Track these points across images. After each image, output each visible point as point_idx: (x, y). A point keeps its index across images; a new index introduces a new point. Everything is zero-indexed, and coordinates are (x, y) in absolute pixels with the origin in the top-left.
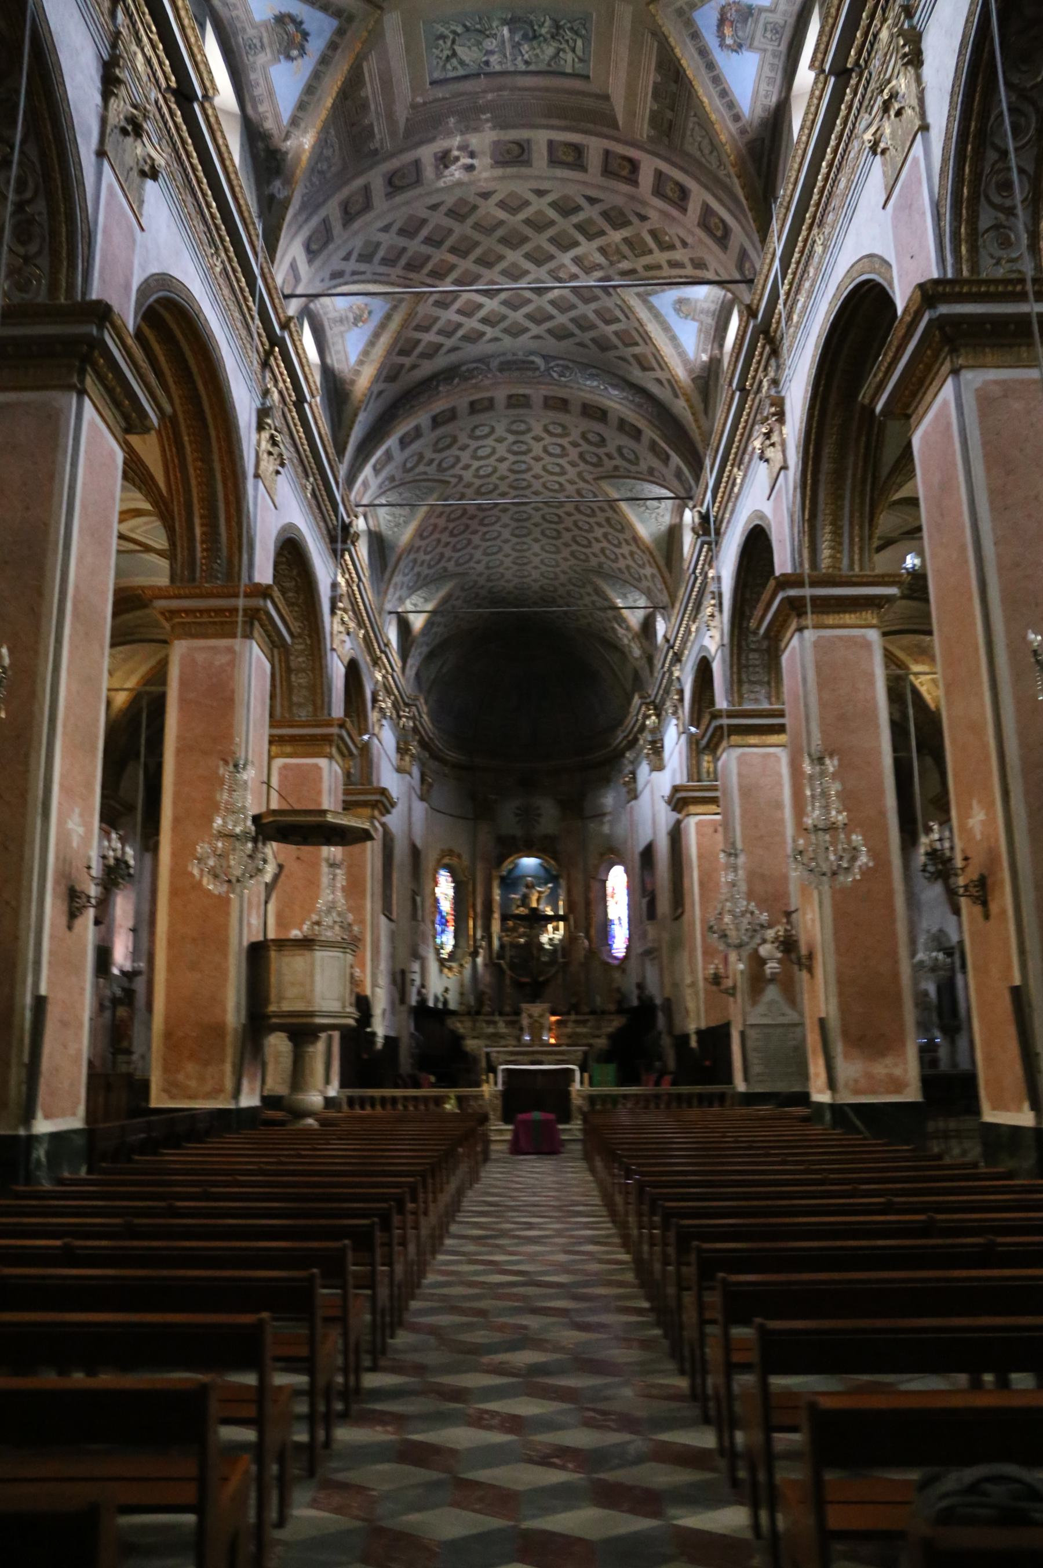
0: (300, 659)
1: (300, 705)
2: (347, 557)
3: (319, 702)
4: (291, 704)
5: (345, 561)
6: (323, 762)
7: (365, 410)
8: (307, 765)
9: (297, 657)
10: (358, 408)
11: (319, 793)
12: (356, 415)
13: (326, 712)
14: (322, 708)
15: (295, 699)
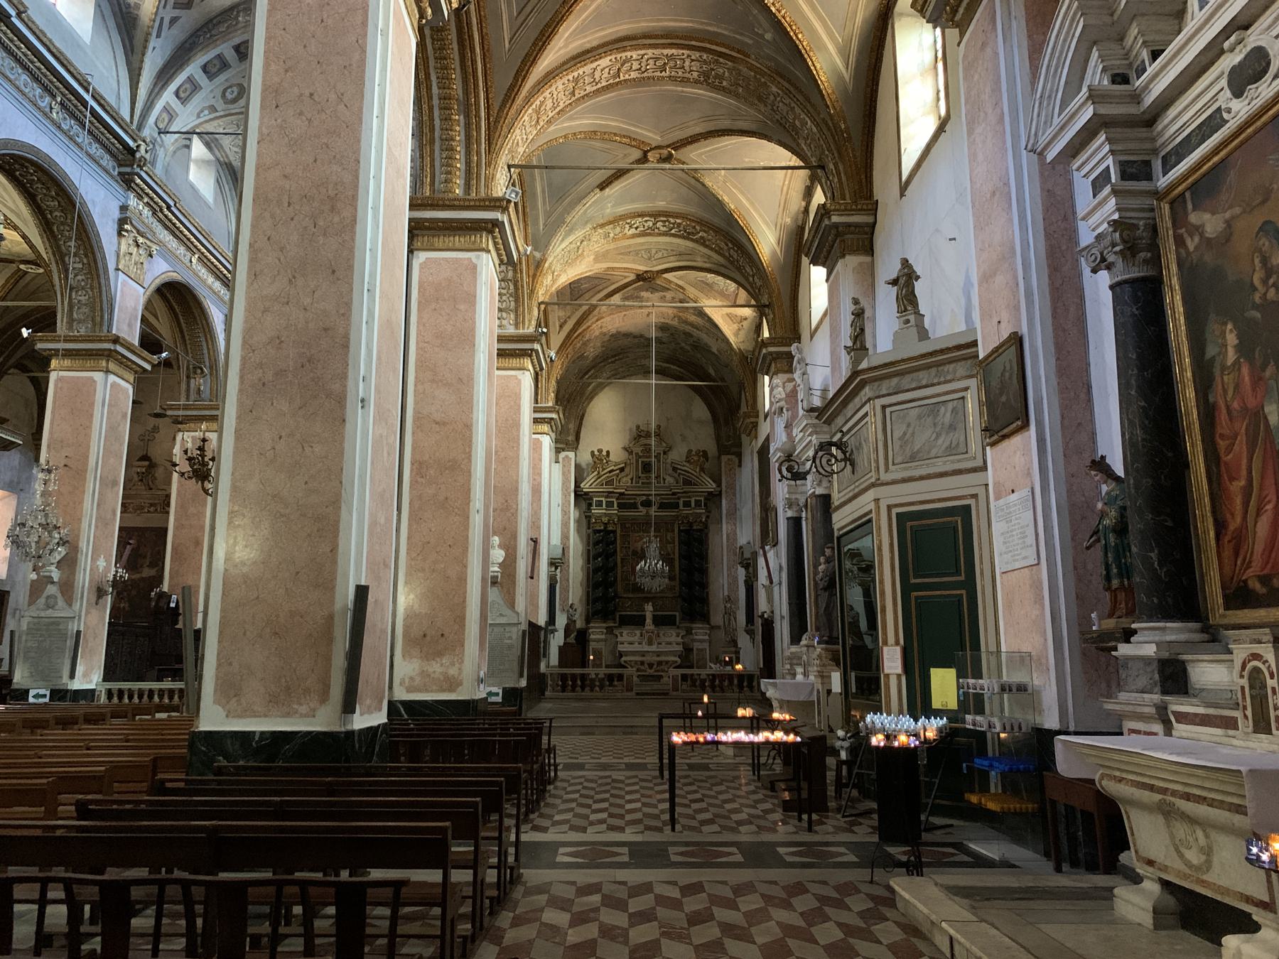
0: (79, 277)
1: (79, 321)
2: (138, 181)
3: (98, 319)
4: (71, 321)
5: (137, 185)
6: (98, 376)
7: (158, 36)
8: (82, 377)
9: (76, 275)
10: (149, 34)
11: (92, 404)
12: (146, 41)
13: (105, 328)
14: (101, 324)
15: (75, 316)
